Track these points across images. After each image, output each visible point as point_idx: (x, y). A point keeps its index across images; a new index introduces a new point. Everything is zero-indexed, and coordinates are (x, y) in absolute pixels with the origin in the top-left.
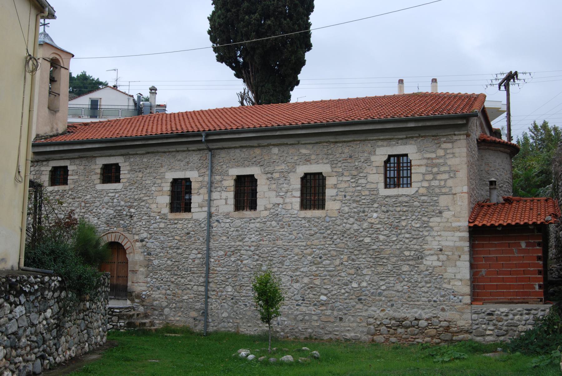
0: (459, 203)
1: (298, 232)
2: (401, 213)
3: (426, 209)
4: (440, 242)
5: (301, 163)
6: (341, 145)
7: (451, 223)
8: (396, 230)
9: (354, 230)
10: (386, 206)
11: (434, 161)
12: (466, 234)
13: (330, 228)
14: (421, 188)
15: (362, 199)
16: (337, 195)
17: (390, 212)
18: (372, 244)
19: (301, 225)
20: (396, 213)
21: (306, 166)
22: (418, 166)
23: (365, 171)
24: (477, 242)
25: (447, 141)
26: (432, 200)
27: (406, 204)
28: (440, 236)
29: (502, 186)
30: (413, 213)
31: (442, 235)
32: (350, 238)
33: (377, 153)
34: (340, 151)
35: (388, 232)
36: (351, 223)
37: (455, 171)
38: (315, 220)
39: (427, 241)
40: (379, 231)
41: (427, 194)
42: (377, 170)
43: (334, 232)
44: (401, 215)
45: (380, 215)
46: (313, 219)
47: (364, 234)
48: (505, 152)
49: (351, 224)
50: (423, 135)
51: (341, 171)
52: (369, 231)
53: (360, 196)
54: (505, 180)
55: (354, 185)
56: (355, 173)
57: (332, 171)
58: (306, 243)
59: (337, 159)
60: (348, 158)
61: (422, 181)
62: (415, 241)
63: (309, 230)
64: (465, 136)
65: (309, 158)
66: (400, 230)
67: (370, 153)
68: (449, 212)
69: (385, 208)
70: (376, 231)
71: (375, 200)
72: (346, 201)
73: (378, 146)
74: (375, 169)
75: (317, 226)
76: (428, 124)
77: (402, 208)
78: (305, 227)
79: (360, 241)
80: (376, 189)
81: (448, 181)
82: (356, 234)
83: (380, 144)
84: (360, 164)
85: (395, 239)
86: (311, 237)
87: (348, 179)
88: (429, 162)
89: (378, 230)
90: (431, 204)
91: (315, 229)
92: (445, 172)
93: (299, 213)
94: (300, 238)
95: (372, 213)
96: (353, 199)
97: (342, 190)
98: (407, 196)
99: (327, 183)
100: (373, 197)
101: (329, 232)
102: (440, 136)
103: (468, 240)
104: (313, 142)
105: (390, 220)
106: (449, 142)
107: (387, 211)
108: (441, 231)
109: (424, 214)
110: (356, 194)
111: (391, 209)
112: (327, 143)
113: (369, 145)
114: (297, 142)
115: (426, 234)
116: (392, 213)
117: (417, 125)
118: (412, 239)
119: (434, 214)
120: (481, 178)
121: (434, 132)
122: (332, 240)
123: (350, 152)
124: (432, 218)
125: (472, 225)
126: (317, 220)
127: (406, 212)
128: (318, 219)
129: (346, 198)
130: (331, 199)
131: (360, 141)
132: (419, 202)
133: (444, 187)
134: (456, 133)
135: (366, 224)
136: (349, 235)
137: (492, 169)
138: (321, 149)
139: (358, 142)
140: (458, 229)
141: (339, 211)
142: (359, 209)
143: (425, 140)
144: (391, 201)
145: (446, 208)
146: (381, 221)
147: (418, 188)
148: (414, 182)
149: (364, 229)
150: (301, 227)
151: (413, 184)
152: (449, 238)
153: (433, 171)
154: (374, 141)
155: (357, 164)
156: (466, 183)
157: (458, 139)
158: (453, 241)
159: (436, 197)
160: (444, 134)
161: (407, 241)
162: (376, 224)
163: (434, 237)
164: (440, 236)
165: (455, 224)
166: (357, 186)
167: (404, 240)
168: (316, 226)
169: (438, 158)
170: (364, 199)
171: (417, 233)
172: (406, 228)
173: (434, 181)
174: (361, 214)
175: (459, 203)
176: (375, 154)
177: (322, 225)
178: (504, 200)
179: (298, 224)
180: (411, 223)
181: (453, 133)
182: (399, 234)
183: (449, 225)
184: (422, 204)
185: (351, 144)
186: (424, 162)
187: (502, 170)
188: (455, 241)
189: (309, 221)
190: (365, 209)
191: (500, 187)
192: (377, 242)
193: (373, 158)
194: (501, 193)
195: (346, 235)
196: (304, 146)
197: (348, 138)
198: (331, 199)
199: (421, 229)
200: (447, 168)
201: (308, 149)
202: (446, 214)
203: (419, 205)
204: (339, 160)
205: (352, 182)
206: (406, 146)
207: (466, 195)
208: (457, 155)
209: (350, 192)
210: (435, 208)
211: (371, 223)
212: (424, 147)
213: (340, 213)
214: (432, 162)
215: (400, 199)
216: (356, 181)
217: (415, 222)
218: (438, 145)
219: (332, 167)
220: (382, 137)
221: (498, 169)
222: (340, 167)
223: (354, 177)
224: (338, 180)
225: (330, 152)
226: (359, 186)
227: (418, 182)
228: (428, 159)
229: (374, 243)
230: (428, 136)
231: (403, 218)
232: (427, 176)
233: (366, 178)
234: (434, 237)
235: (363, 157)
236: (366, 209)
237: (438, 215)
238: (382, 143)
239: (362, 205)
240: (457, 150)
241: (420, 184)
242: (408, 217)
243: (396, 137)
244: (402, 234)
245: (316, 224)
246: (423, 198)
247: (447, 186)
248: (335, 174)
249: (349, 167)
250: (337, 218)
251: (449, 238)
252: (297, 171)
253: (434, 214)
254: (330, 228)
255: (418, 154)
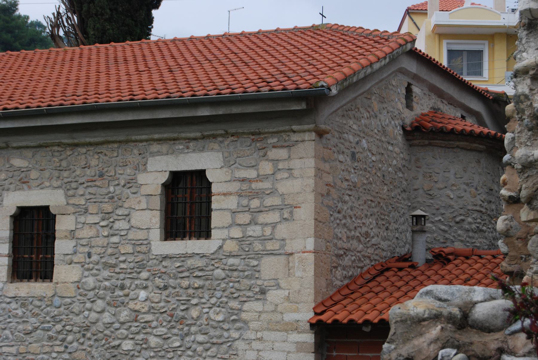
0: (298, 274)
1: (3, 327)
2: (191, 291)
3: (236, 285)
4: (261, 353)
5: (12, 186)
6: (84, 150)
7: (282, 313)
8: (181, 326)
9: (104, 324)
10: (164, 276)
11: (254, 186)
12: (309, 338)
13: (61, 320)
14: (228, 241)
15: (121, 262)
16: (75, 253)
17: (170, 289)
18: (137, 354)
19: (10, 312)
20: (181, 291)
21: (21, 192)
22: (225, 194)
23: (126, 205)
24: (335, 354)
25: (279, 144)
26: (248, 266)
27: (200, 274)
28: (260, 339)
29: (463, 220)
30: (212, 292)
31: (265, 338)
32: (96, 340)
33: (149, 168)
34: (83, 163)
35: (165, 330)
36: (99, 310)
37: (291, 206)
38: (34, 303)
39: (237, 349)
40: (150, 327)
41: (240, 253)
42: (147, 203)
43: (68, 328)
44: (190, 296)
45: (152, 294)
46: (31, 299)
47: (121, 333)
48: (471, 150)
49: (98, 312)
50: (233, 131)
51: (84, 203)
52: (130, 327)
53: (117, 256)
54: (470, 207)
55: (106, 234)
56: (108, 207)
57: (68, 204)
58: (18, 349)
59: (77, 178)
60: (97, 177)
61: (230, 226)
62: (214, 349)
63: (24, 322)
64: (314, 134)
65: (26, 177)
66: (187, 325)
67: (137, 168)
68: (279, 292)
69: (160, 280)
70: (144, 328)
71: (143, 264)
72: (91, 266)
73: (153, 154)
74: (144, 200)
75: (38, 315)
76: (236, 110)
77: (193, 280)
78: (16, 316)
79: (113, 347)
80: (145, 242)
81: (279, 226)
82: (107, 332)
83: (155, 150)
84: (118, 190)
85: (177, 344)
86: (28, 338)
87: (96, 219)
88: (245, 186)
89: (147, 325)
90: (246, 273)
91: (33, 320)
92: (272, 208)
93: (5, 288)
94: (7, 338)
95: (137, 291)
96: (103, 260)
97: (84, 242)
98: (203, 256)
99: (57, 228)
100: (140, 257)
101: (59, 327)
102: (266, 133)
103: (313, 351)
104: (32, 144)
105: (169, 304)
106: (282, 147)
107: (165, 288)
108: (262, 330)
109: (232, 293)
110: (110, 251)
111: (172, 282)
112: (59, 146)
113: (136, 151)
114: (4, 145)
115: (235, 335)
116: (173, 291)
117: (214, 113)
118: (209, 345)
119: (250, 294)
120: (414, 205)
121: (253, 127)
122: (65, 344)
123: (100, 166)
124: (247, 304)
125: (314, 321)
126: (38, 303)
127: (200, 290)
128: (40, 300)
129: (91, 260)
130: (63, 261)
131: (120, 142)
132: (224, 270)
133: (272, 239)
134: (295, 127)
135: (126, 313)
136: (94, 335)
137: (441, 185)
138: (48, 158)
139: (116, 145)
140: (294, 327)
141: (78, 284)
142: (114, 280)
143: (238, 142)
144: (172, 266)
145: (272, 283)
146: (153, 308)
147: (224, 240)
148: (215, 228)
149: (123, 323)
150: (9, 317)
151: (213, 232)
152: (277, 344)
153: (252, 207)
154: (145, 143)
155: (112, 189)
156: (312, 232)
157: (300, 139)
158: (284, 351)
159: (256, 259)
160: (271, 130)
161: (200, 349)
162: (144, 313)
163: (249, 342)
164: (260, 339)
165: (289, 317)
166: (112, 235)
167: (194, 346)
168: (36, 315)
169: (260, 178)
170: (124, 261)
171: (218, 333)
172: (198, 323)
173: (253, 227)
174: (119, 293)
175: (298, 274)
176: (145, 171)
177: (47, 314)
178: (434, 256)
179: (4, 309)
180: (207, 313)
181: (287, 128)
182: (187, 335)
183: (278, 317)
184: (230, 274)
185: (103, 149)
186: (235, 187)
187: (465, 187)
188: (289, 352)
189: (23, 305)
190: (125, 282)
191: (457, 223)
192: (146, 349)
193: (142, 178)
194: (459, 235)
195: (89, 335)
196: (18, 152)
197: (95, 137)
198: (63, 261)
199: (226, 326)
200: (276, 201)
201: (24, 158)
202: (273, 295)
203: (223, 275)
204: (81, 180)
205: (102, 227)
206: (204, 154)
207: (311, 257)
208: (296, 173)
209: (98, 246)
210: (252, 282)
211: (136, 311)
212: (235, 156)
213: (79, 288)
214: (250, 188)
215: (190, 262)
216: (111, 224)
217: (214, 312)
218: (261, 153)
219: (67, 196)
220: (156, 136)
221: (453, 185)
222: (82, 195)
223: (107, 216)
224: (77, 223)
225: (64, 164)
226: (116, 235)
227: (223, 228)
228: (243, 180)
229: (140, 352)
230: (243, 133)
231: (194, 301)
232: (240, 215)
233: (127, 219)
234: (249, 342)
235: (124, 176)
236: (127, 283)
237: (259, 297)
238: (159, 146)
239: (119, 273)
240: (296, 164)
241: (226, 231)
242: (203, 300)
243: (183, 135)
244: (192, 334)
245: (36, 311)
246: (231, 261)
247: (276, 237)
248: (71, 209)
249: (98, 196)
250: (74, 299)
251: (277, 344)
252: (5, 203)
253: (250, 294)
254: (61, 320)
255: (225, 169)
